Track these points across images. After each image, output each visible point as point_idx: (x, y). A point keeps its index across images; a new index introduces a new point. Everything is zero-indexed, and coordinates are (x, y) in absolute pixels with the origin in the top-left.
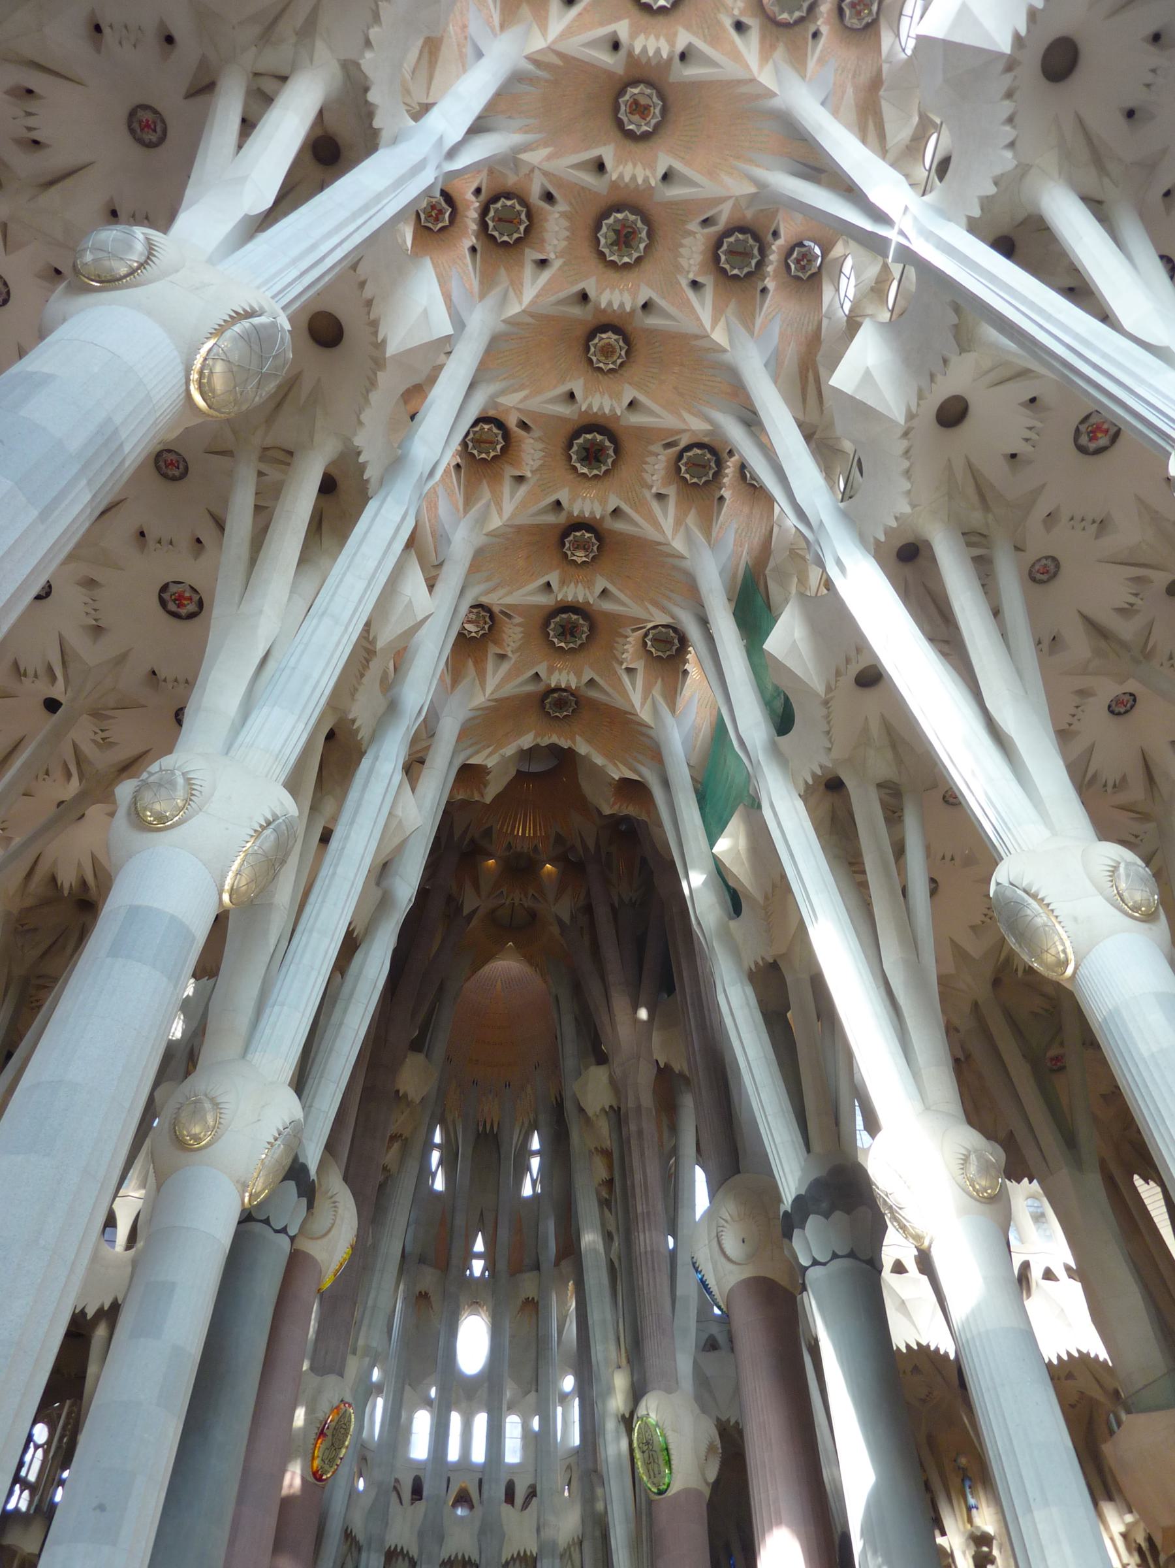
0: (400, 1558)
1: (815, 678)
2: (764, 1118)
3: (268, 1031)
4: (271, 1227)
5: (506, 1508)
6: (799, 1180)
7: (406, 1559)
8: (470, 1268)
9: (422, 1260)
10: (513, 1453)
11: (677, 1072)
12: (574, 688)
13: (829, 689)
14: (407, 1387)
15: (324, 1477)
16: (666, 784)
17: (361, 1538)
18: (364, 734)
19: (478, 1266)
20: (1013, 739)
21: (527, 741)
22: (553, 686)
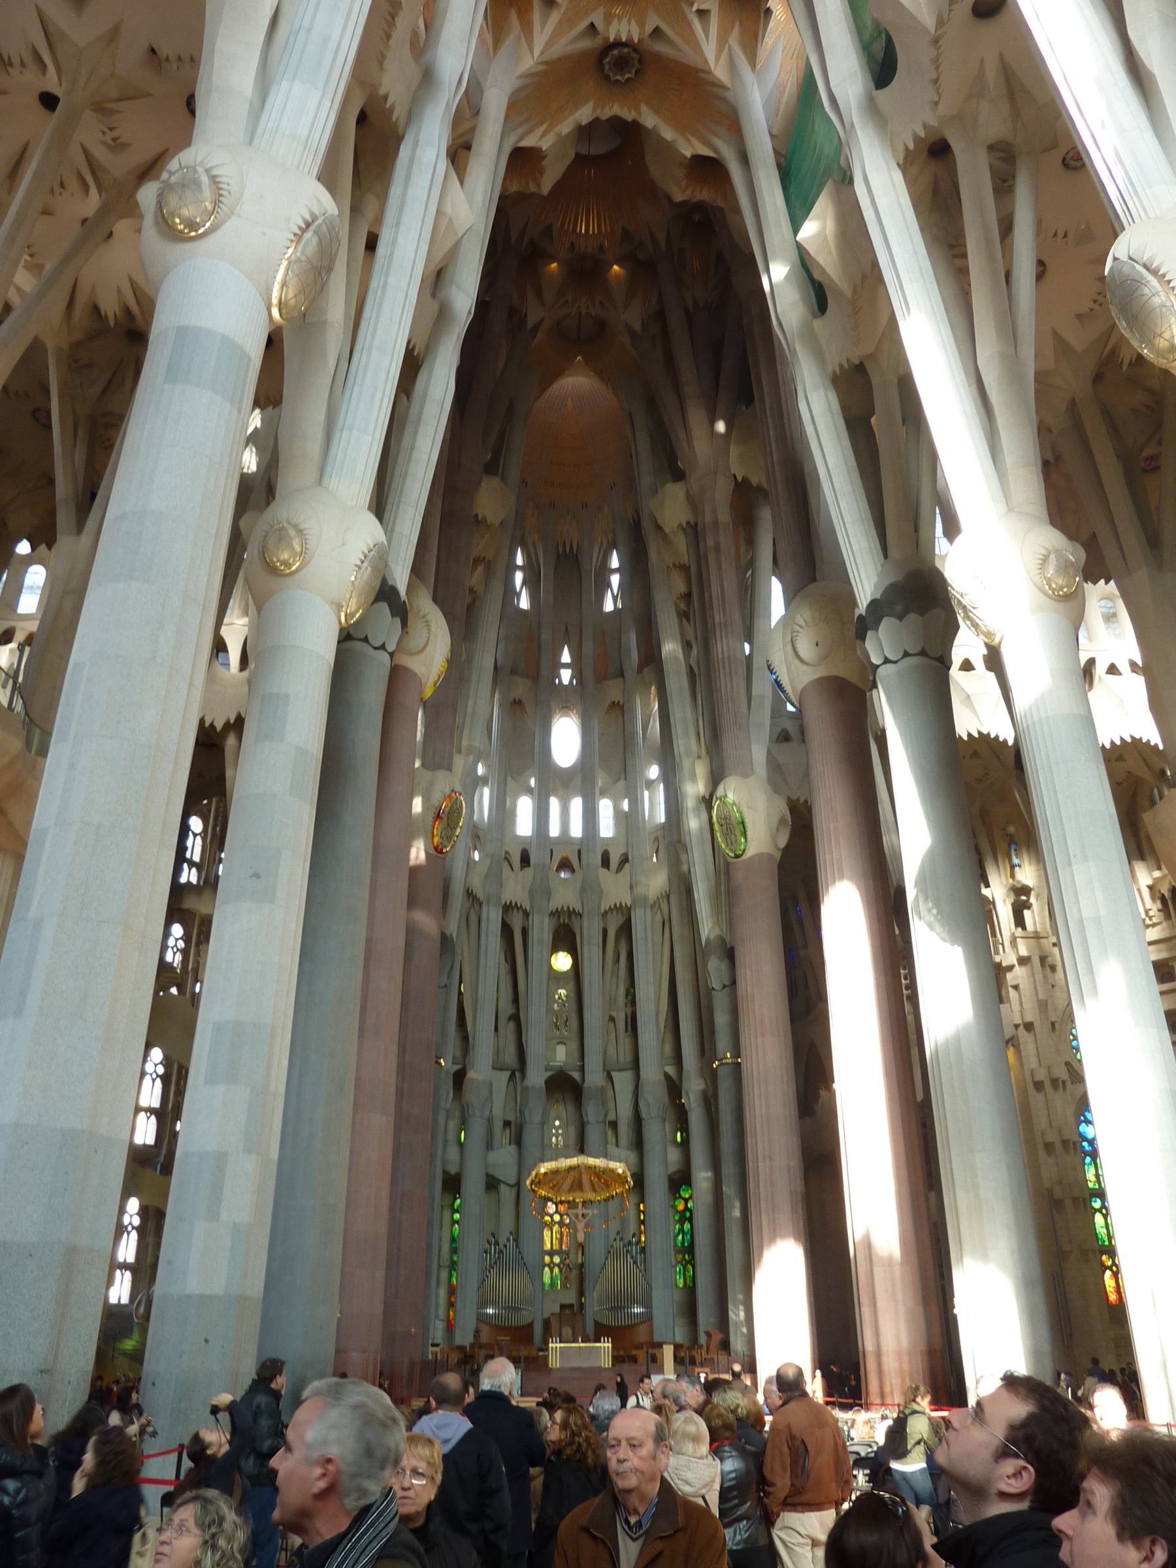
0: (515, 911)
1: (925, 9)
2: (842, 525)
3: (340, 456)
4: (370, 644)
5: (602, 872)
6: (875, 586)
7: (521, 912)
8: (559, 677)
9: (514, 671)
10: (607, 828)
11: (755, 485)
12: (636, 41)
13: (940, 22)
14: (509, 779)
15: (444, 851)
16: (744, 159)
17: (481, 895)
18: (399, 113)
19: (566, 675)
20: (1155, 76)
21: (584, 114)
22: (612, 39)
